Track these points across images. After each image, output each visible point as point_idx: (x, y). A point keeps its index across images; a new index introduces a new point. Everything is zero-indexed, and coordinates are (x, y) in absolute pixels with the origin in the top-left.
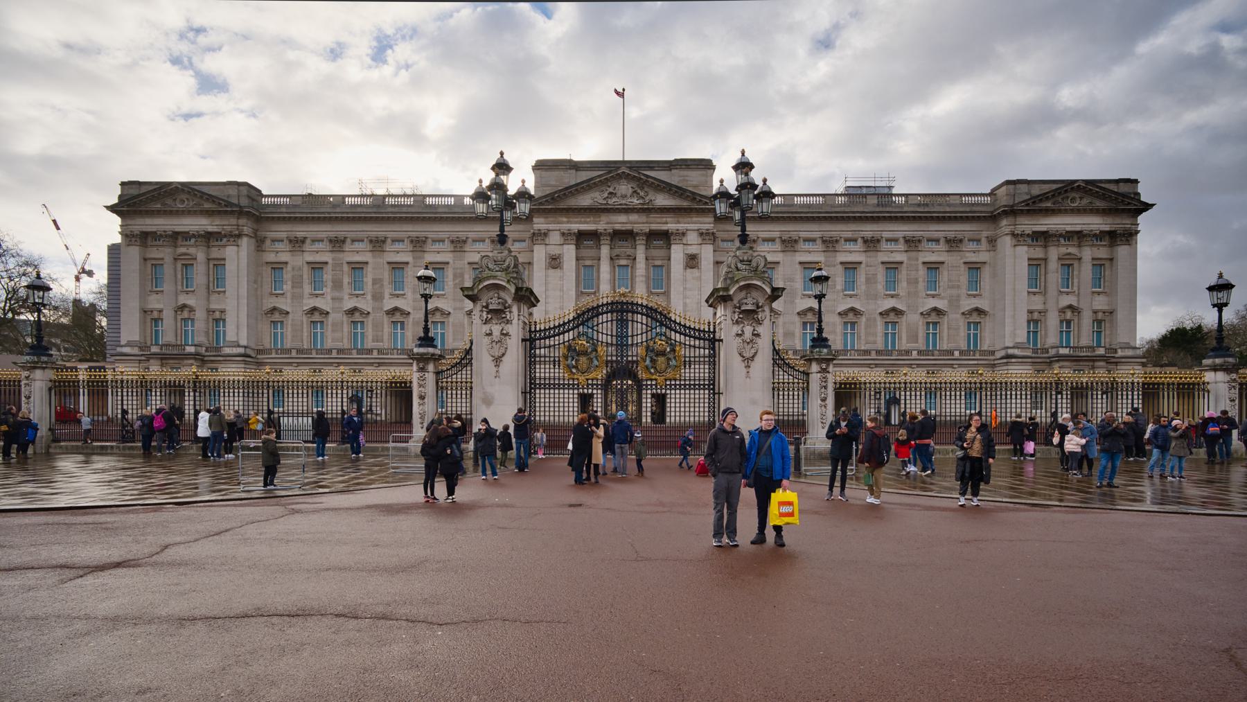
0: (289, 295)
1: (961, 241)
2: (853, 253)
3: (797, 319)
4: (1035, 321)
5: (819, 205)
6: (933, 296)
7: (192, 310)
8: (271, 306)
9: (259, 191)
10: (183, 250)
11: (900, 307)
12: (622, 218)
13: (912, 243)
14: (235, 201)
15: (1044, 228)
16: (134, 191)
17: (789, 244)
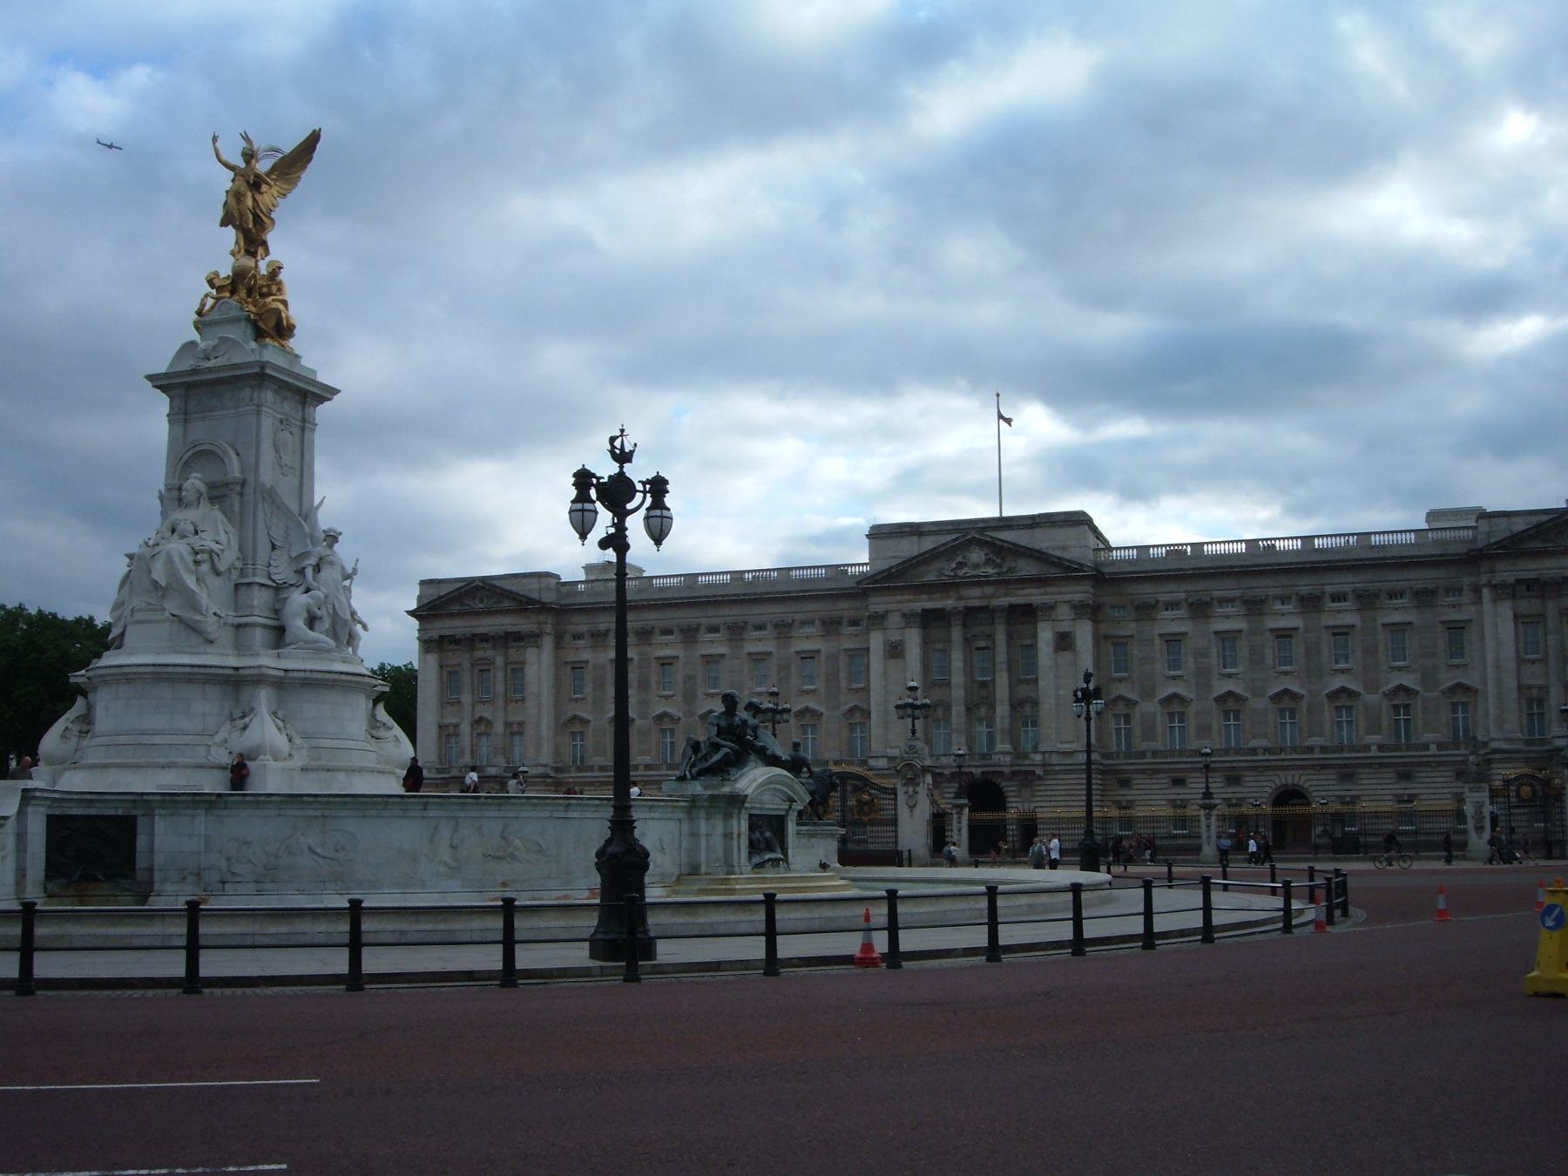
0: (590, 699)
1: (1434, 592)
2: (1286, 617)
3: (1214, 705)
4: (1533, 700)
5: (1238, 555)
6: (1400, 669)
7: (488, 723)
8: (570, 715)
9: (557, 577)
10: (479, 654)
11: (1353, 687)
12: (976, 592)
13: (1366, 600)
14: (535, 596)
15: (1532, 575)
16: (434, 593)
17: (1200, 609)
